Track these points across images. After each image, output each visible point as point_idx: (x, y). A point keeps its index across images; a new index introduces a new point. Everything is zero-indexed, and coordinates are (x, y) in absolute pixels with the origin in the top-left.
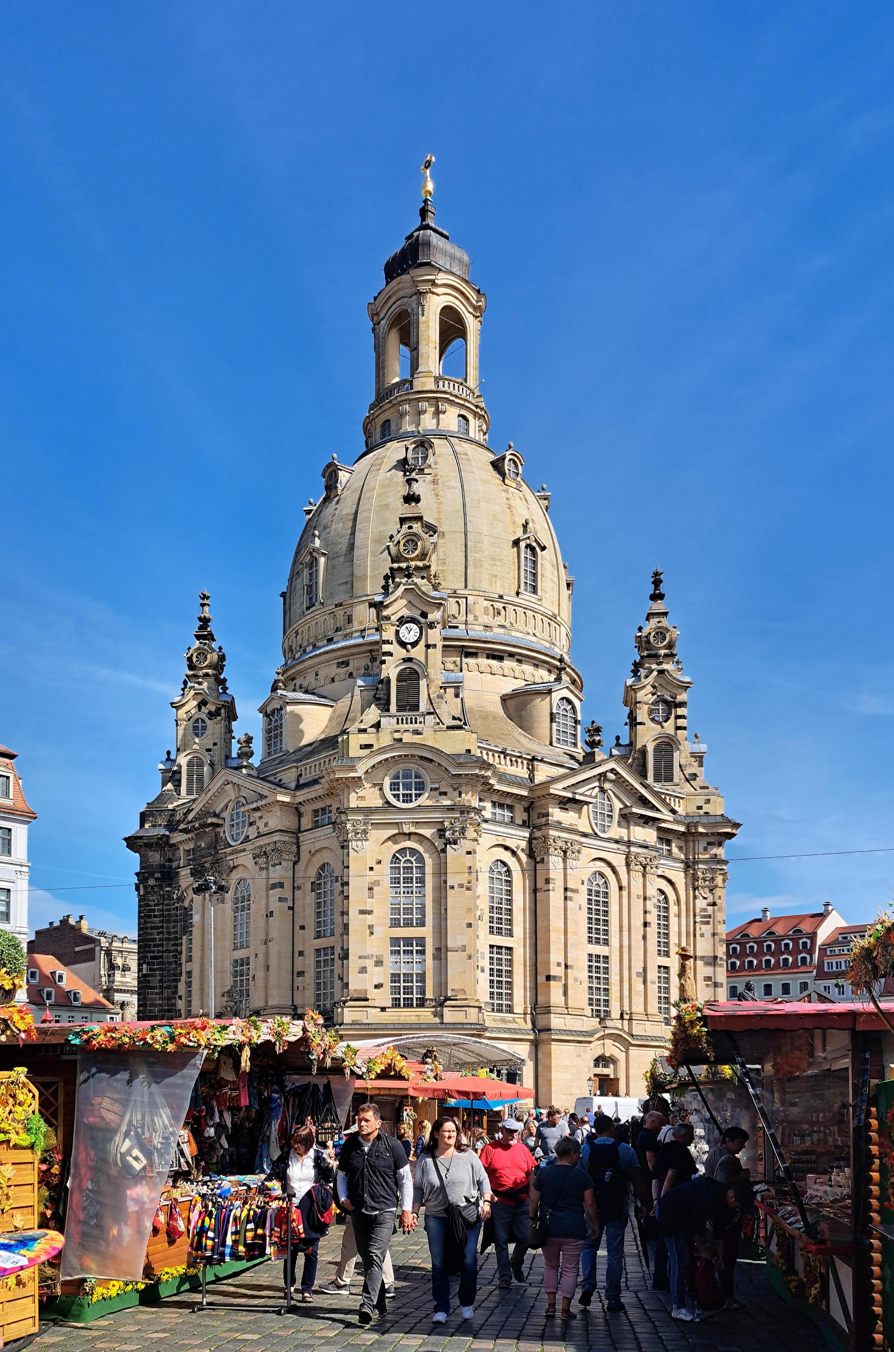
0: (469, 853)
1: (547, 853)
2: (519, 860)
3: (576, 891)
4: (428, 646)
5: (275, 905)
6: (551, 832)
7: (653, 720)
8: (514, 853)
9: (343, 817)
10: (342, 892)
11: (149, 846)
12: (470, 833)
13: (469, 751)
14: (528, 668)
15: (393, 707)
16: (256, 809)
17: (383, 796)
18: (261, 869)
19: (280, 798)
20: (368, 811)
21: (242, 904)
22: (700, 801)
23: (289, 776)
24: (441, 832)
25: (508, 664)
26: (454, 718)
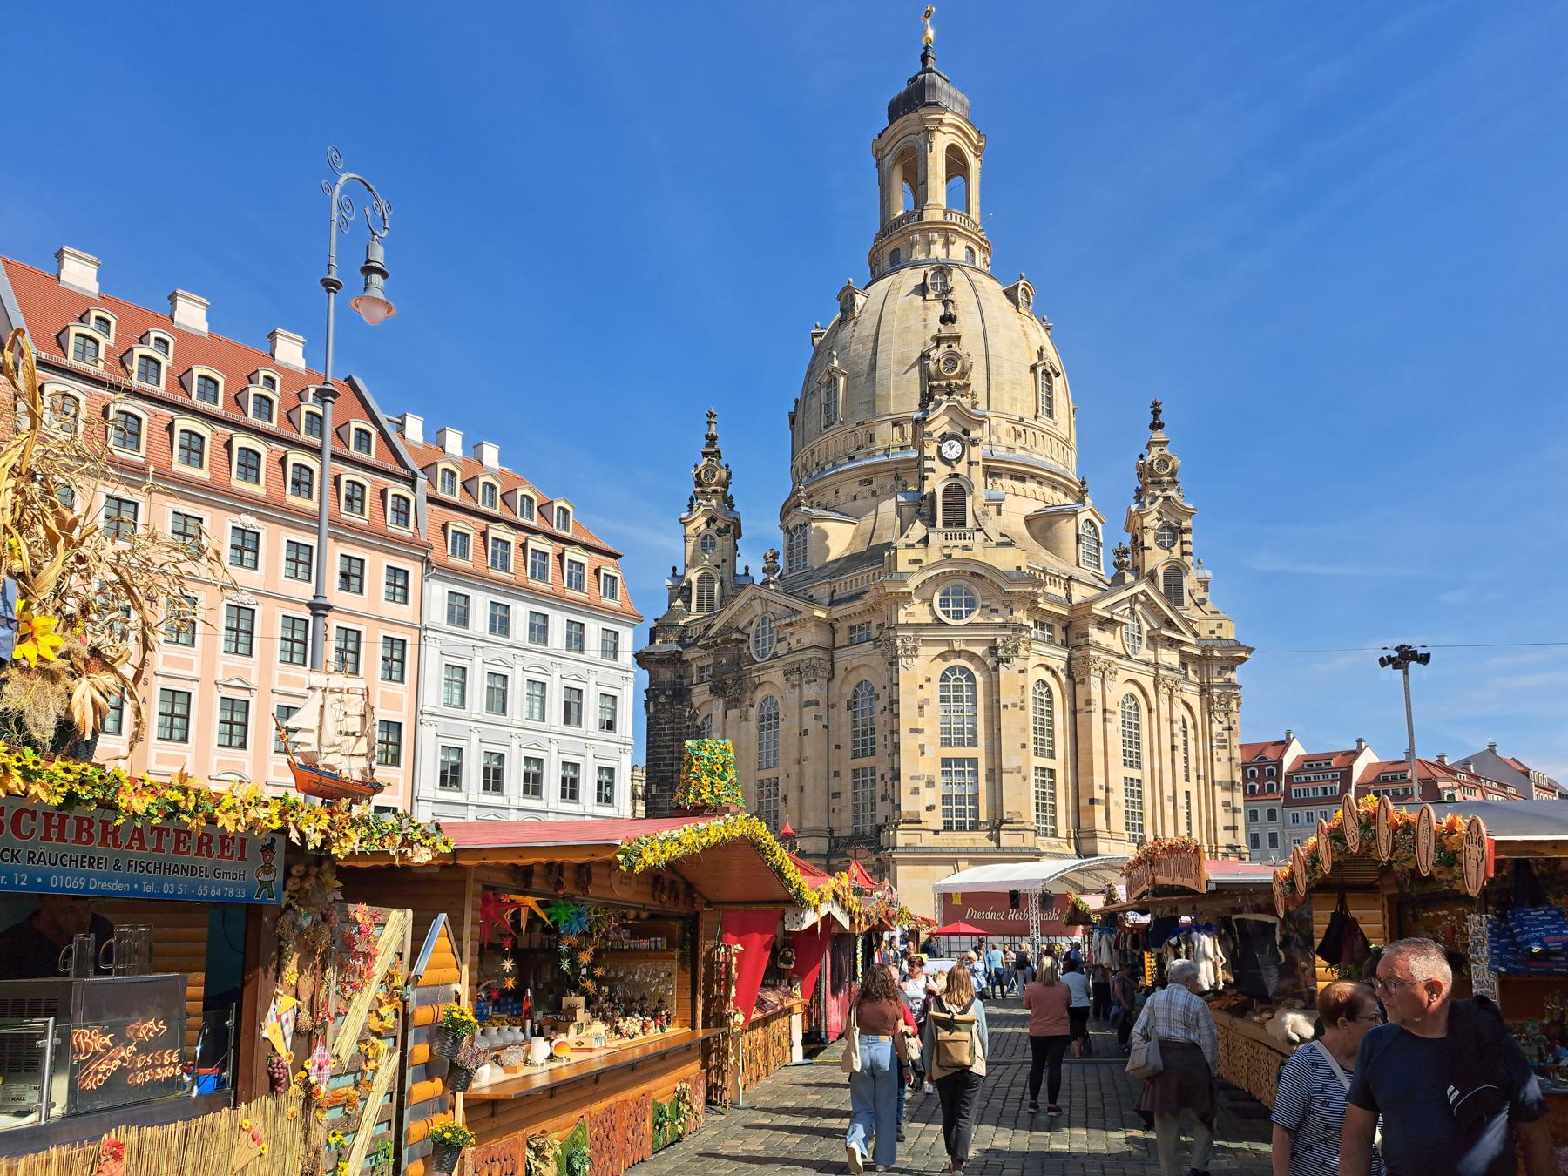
0: (1022, 672)
1: (1088, 673)
2: (1059, 680)
3: (1113, 713)
4: (970, 463)
5: (809, 722)
6: (1092, 653)
7: (1161, 545)
8: (1054, 673)
9: (892, 633)
11: (660, 662)
12: (1022, 652)
13: (1019, 568)
14: (1048, 490)
15: (939, 523)
16: (790, 625)
17: (933, 612)
18: (793, 686)
19: (817, 613)
20: (918, 627)
21: (769, 720)
22: (1213, 625)
23: (822, 592)
24: (993, 650)
25: (1031, 486)
26: (1002, 535)
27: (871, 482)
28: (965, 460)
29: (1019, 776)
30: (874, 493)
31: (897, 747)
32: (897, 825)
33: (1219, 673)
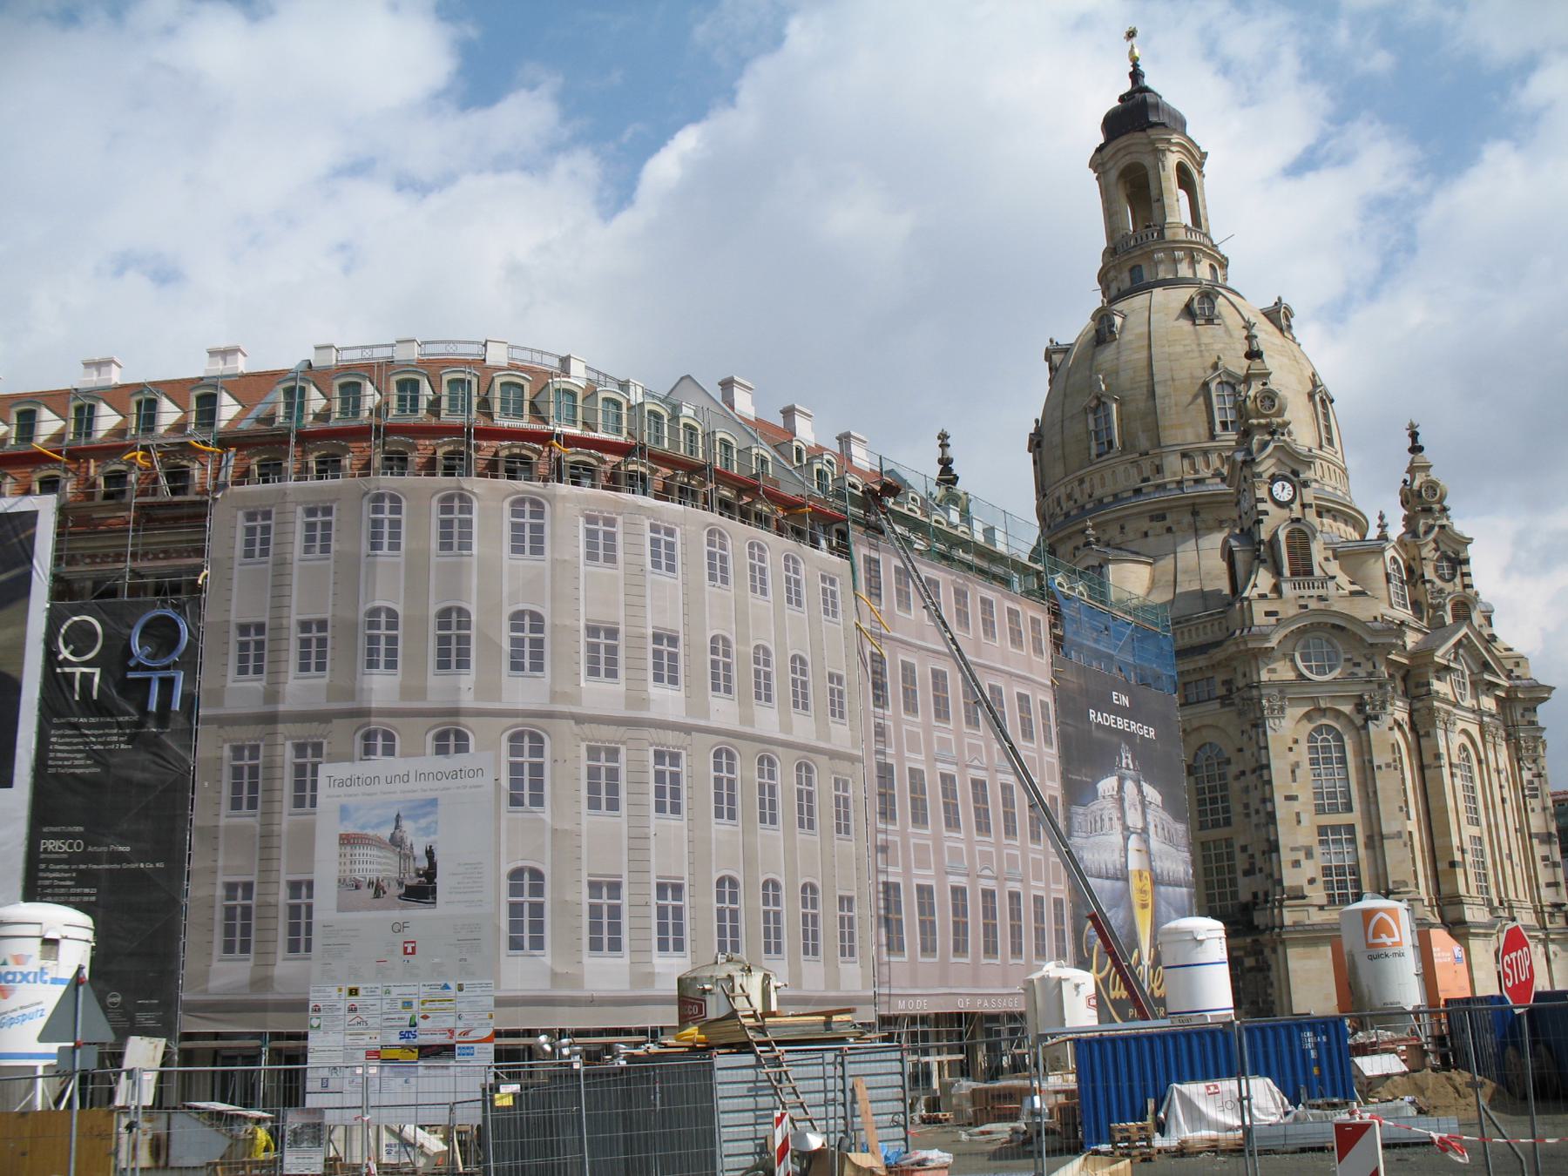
3: (1457, 766)
4: (1304, 506)
9: (1255, 692)
15: (1286, 572)
17: (1295, 668)
20: (1283, 686)
24: (1360, 706)
27: (1163, 518)
28: (1298, 502)
29: (1401, 842)
30: (1169, 530)
31: (1272, 817)
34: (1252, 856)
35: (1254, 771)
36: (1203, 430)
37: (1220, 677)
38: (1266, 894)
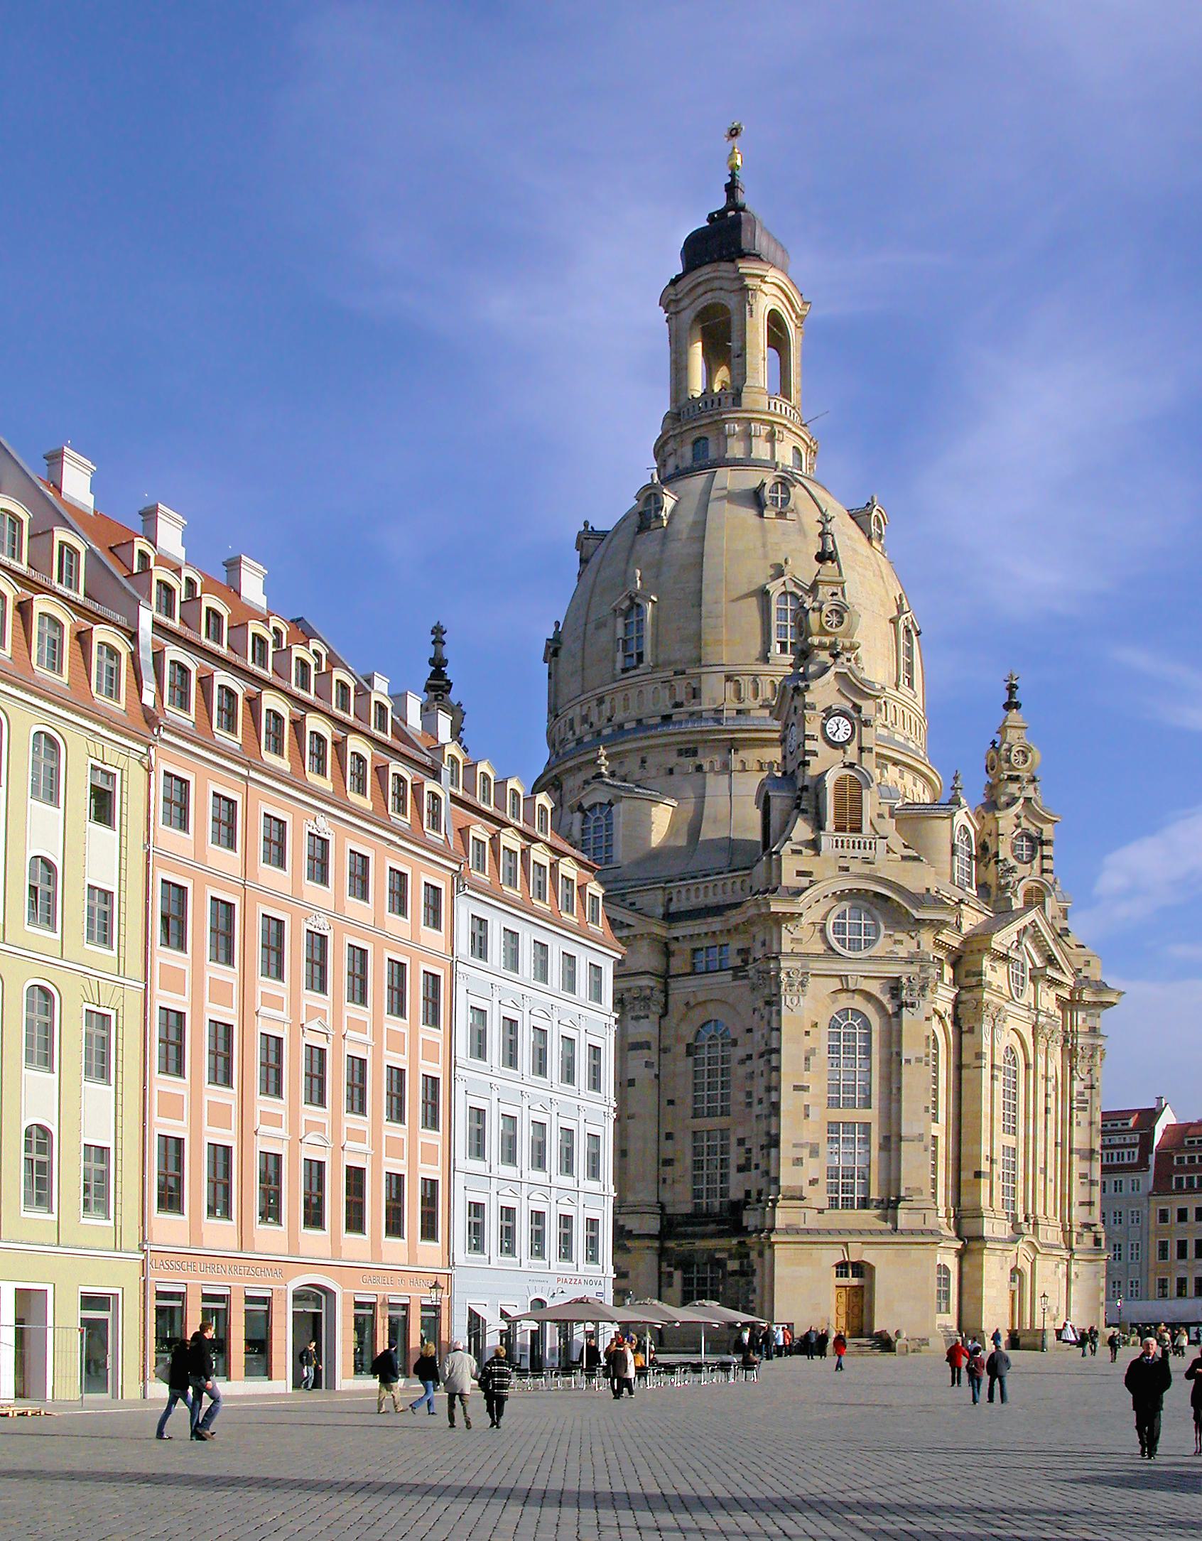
1: (980, 1020)
3: (999, 1068)
4: (861, 749)
8: (941, 1018)
10: (769, 1061)
12: (928, 993)
15: (830, 825)
17: (825, 940)
28: (855, 744)
31: (776, 1107)
32: (775, 1201)
33: (1084, 1021)
34: (749, 1151)
35: (761, 1056)
36: (756, 649)
37: (736, 944)
38: (760, 1193)
